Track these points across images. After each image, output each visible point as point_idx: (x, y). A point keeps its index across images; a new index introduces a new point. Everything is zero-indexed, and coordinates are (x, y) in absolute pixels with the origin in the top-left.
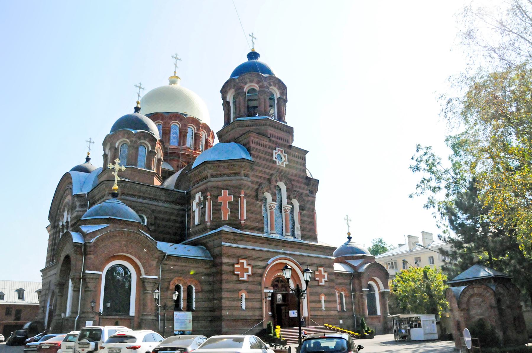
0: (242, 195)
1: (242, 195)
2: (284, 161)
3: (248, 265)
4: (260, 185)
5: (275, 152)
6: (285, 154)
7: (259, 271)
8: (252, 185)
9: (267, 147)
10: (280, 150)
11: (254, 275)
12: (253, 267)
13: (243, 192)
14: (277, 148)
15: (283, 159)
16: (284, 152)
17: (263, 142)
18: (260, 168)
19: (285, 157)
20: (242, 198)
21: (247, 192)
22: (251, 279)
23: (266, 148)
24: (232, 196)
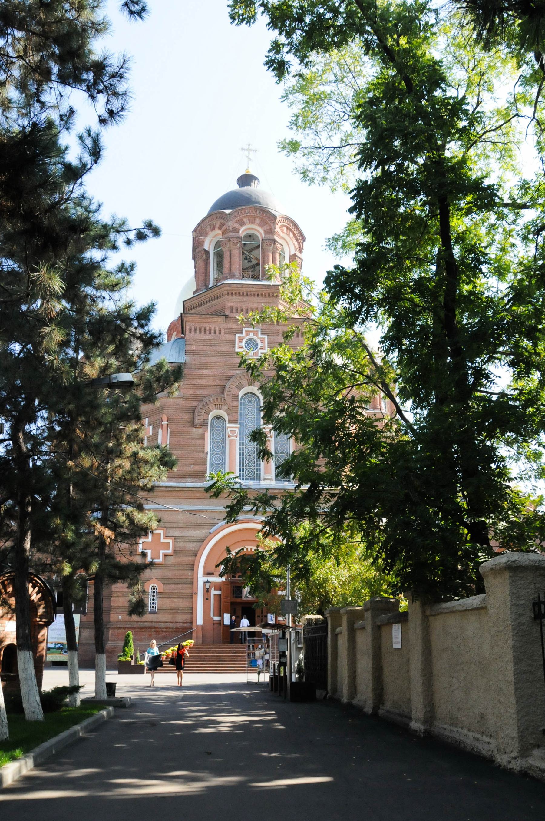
0: (165, 422)
1: (165, 422)
2: (262, 348)
3: (166, 537)
4: (201, 399)
5: (239, 337)
6: (263, 336)
7: (191, 546)
8: (185, 403)
9: (223, 332)
10: (252, 331)
11: (176, 553)
12: (176, 540)
13: (165, 417)
14: (244, 329)
15: (260, 345)
16: (260, 333)
17: (213, 326)
18: (199, 372)
19: (262, 340)
20: (165, 427)
21: (173, 415)
22: (171, 560)
23: (220, 333)
24: (151, 427)
